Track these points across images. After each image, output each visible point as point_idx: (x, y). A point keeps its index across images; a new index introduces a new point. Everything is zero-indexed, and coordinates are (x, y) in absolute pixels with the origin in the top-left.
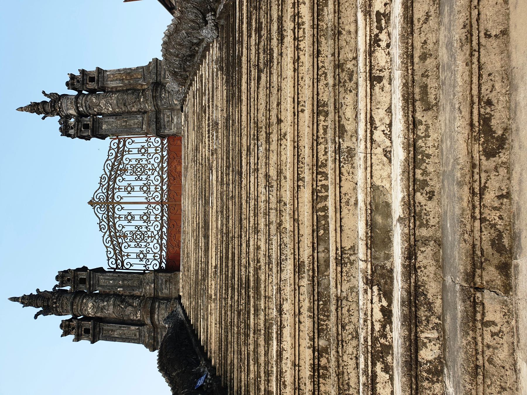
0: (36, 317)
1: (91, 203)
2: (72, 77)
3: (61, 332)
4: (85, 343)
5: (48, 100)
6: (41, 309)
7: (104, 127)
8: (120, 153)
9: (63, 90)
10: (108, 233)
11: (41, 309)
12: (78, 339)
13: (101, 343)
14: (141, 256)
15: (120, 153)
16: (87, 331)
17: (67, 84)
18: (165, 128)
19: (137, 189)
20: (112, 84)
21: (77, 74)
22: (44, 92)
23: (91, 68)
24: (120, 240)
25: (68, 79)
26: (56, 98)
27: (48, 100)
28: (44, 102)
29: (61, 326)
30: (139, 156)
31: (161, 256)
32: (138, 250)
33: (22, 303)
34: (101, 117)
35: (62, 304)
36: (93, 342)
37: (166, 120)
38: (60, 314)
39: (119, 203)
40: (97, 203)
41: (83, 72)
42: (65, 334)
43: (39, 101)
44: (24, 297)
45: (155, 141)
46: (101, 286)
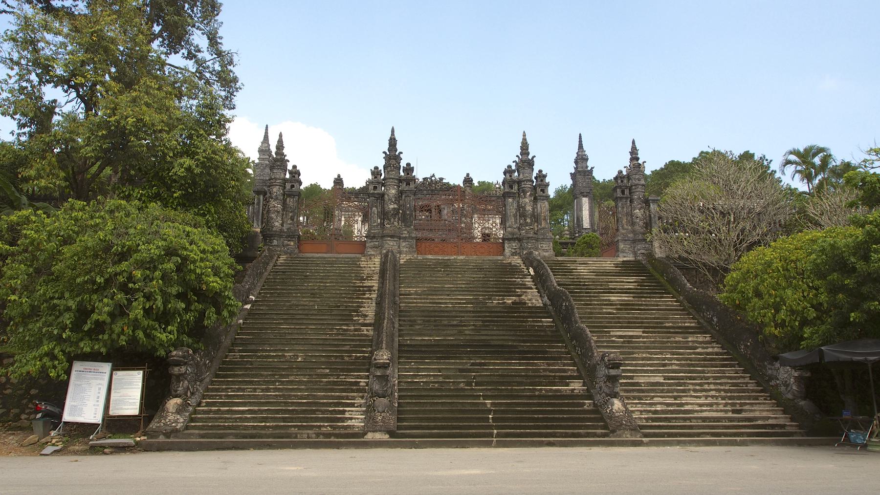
0: (384, 152)
2: (545, 176)
5: (530, 157)
6: (388, 153)
7: (510, 200)
18: (508, 244)
21: (547, 180)
22: (535, 156)
25: (544, 173)
26: (530, 164)
28: (528, 154)
33: (391, 139)
35: (393, 171)
37: (514, 244)
38: (385, 167)
42: (373, 173)
44: (395, 139)
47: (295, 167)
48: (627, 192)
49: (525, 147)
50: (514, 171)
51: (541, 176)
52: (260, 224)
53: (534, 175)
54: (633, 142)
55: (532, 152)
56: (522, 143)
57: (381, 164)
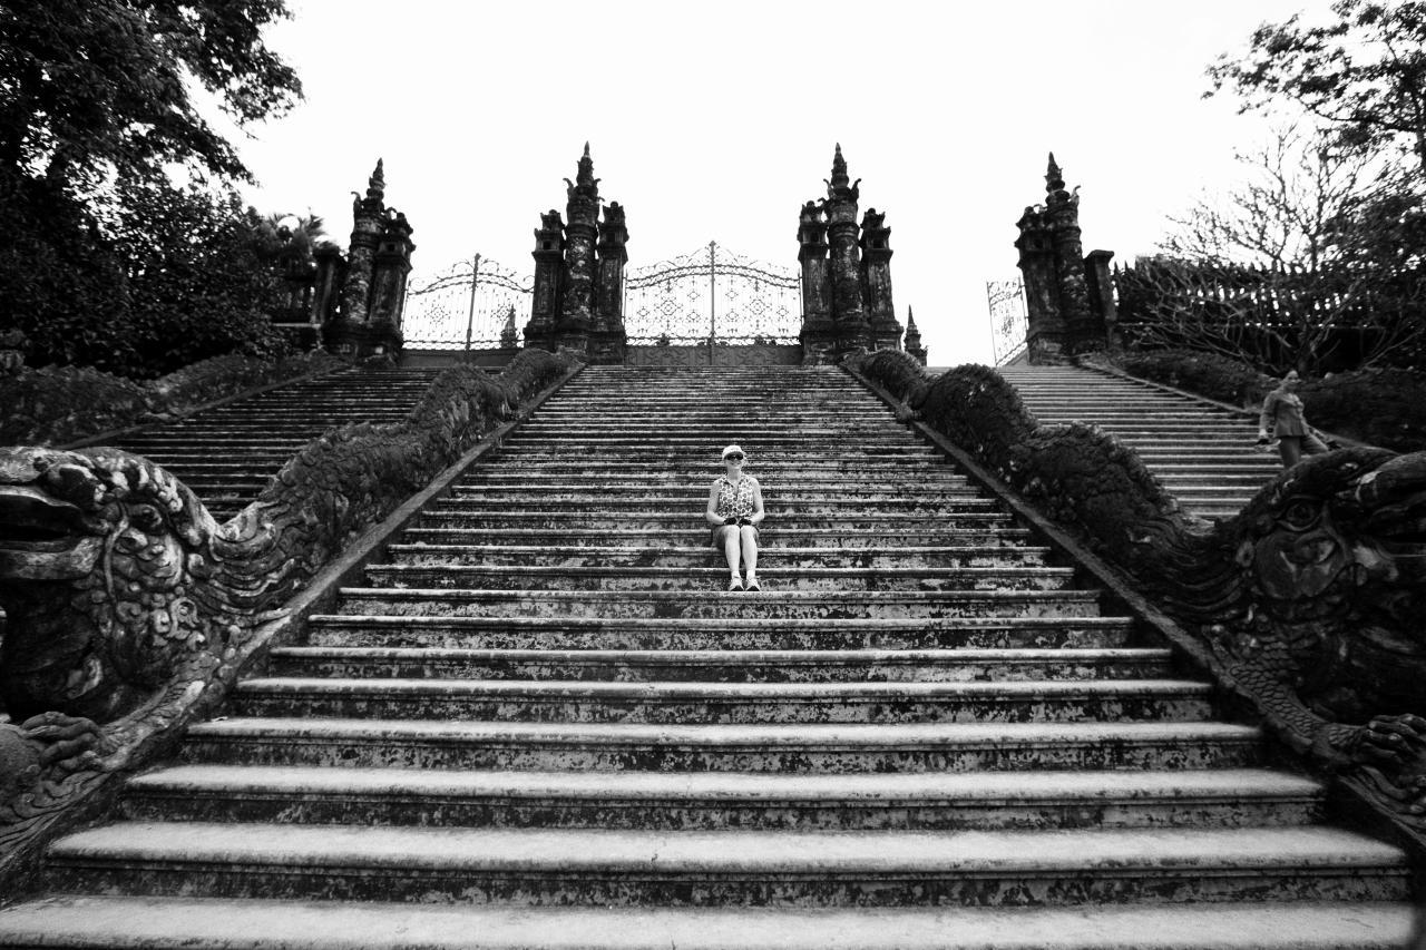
1: (712, 244)
2: (882, 217)
3: (547, 213)
4: (532, 244)
5: (850, 186)
7: (814, 262)
8: (776, 281)
9: (863, 205)
10: (673, 267)
11: (575, 184)
12: (539, 235)
13: (533, 263)
14: (643, 313)
15: (776, 281)
16: (547, 246)
17: (872, 211)
19: (732, 305)
20: (871, 271)
21: (885, 225)
23: (893, 242)
24: (664, 284)
25: (878, 212)
26: (853, 195)
27: (850, 186)
28: (847, 179)
29: (553, 212)
30: (775, 308)
31: (643, 338)
32: (650, 308)
33: (583, 159)
34: (828, 256)
36: (534, 254)
38: (570, 208)
39: (713, 280)
40: (712, 253)
41: (888, 231)
42: (544, 218)
43: (849, 173)
45: (795, 328)
46: (604, 263)
47: (401, 215)
48: (1047, 245)
49: (840, 167)
50: (819, 210)
51: (874, 219)
52: (322, 316)
53: (859, 220)
54: (1051, 157)
55: (853, 175)
56: (836, 161)
57: (560, 204)
